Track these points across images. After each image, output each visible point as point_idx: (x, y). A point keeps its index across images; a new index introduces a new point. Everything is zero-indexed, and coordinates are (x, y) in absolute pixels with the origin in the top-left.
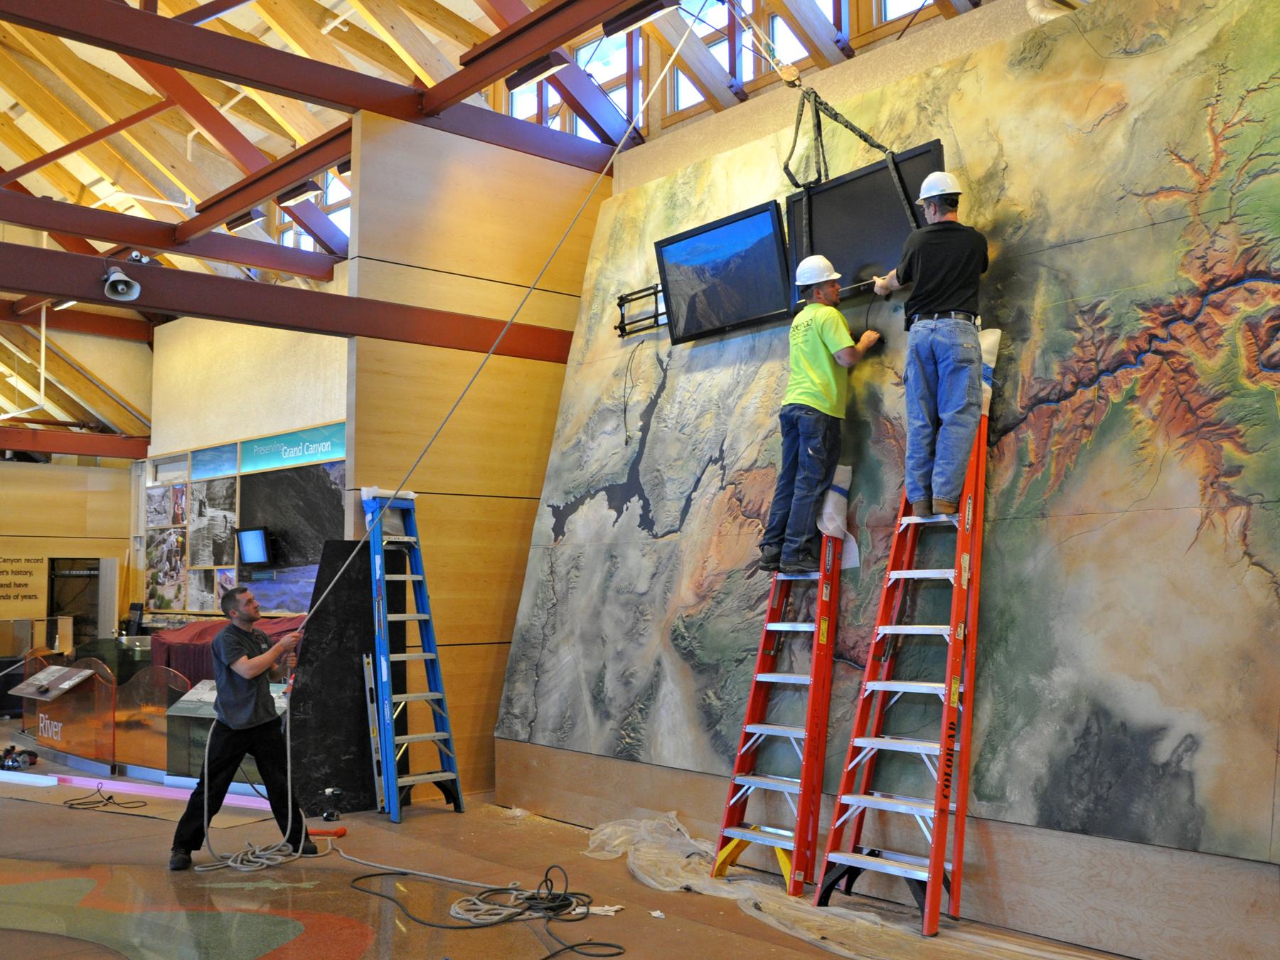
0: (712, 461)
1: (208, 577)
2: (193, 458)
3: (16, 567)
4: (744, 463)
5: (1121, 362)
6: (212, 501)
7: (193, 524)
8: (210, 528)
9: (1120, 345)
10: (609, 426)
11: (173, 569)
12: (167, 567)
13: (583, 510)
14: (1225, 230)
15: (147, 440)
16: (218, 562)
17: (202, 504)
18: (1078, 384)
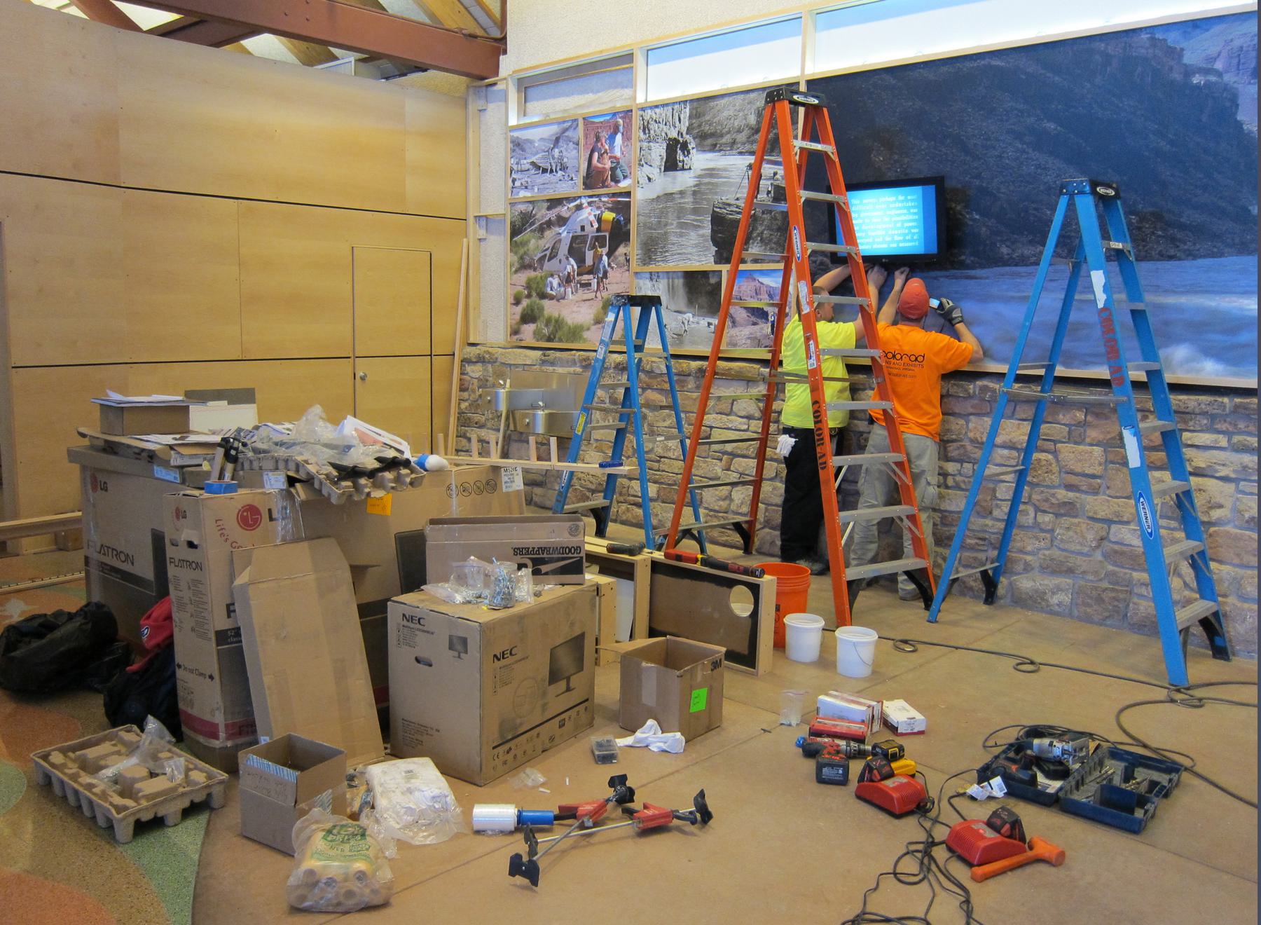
1: (700, 289)
6: (710, 139)
7: (646, 185)
17: (674, 147)
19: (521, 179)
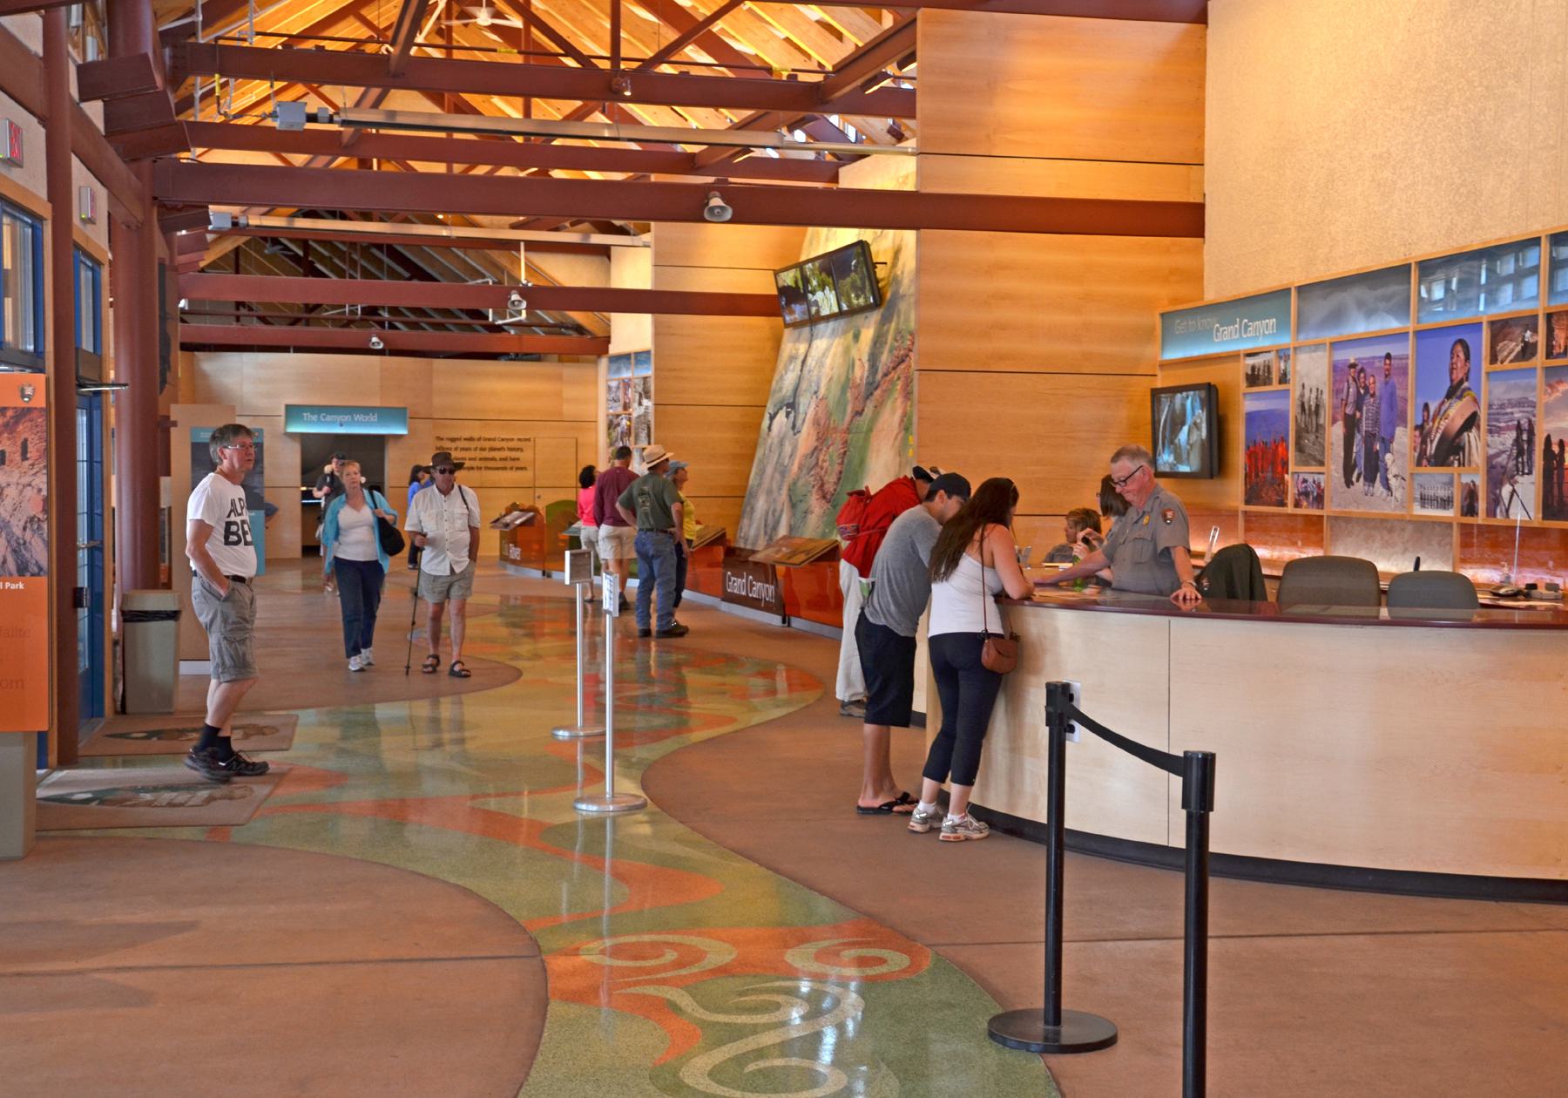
3: (511, 444)
7: (636, 411)
15: (607, 340)
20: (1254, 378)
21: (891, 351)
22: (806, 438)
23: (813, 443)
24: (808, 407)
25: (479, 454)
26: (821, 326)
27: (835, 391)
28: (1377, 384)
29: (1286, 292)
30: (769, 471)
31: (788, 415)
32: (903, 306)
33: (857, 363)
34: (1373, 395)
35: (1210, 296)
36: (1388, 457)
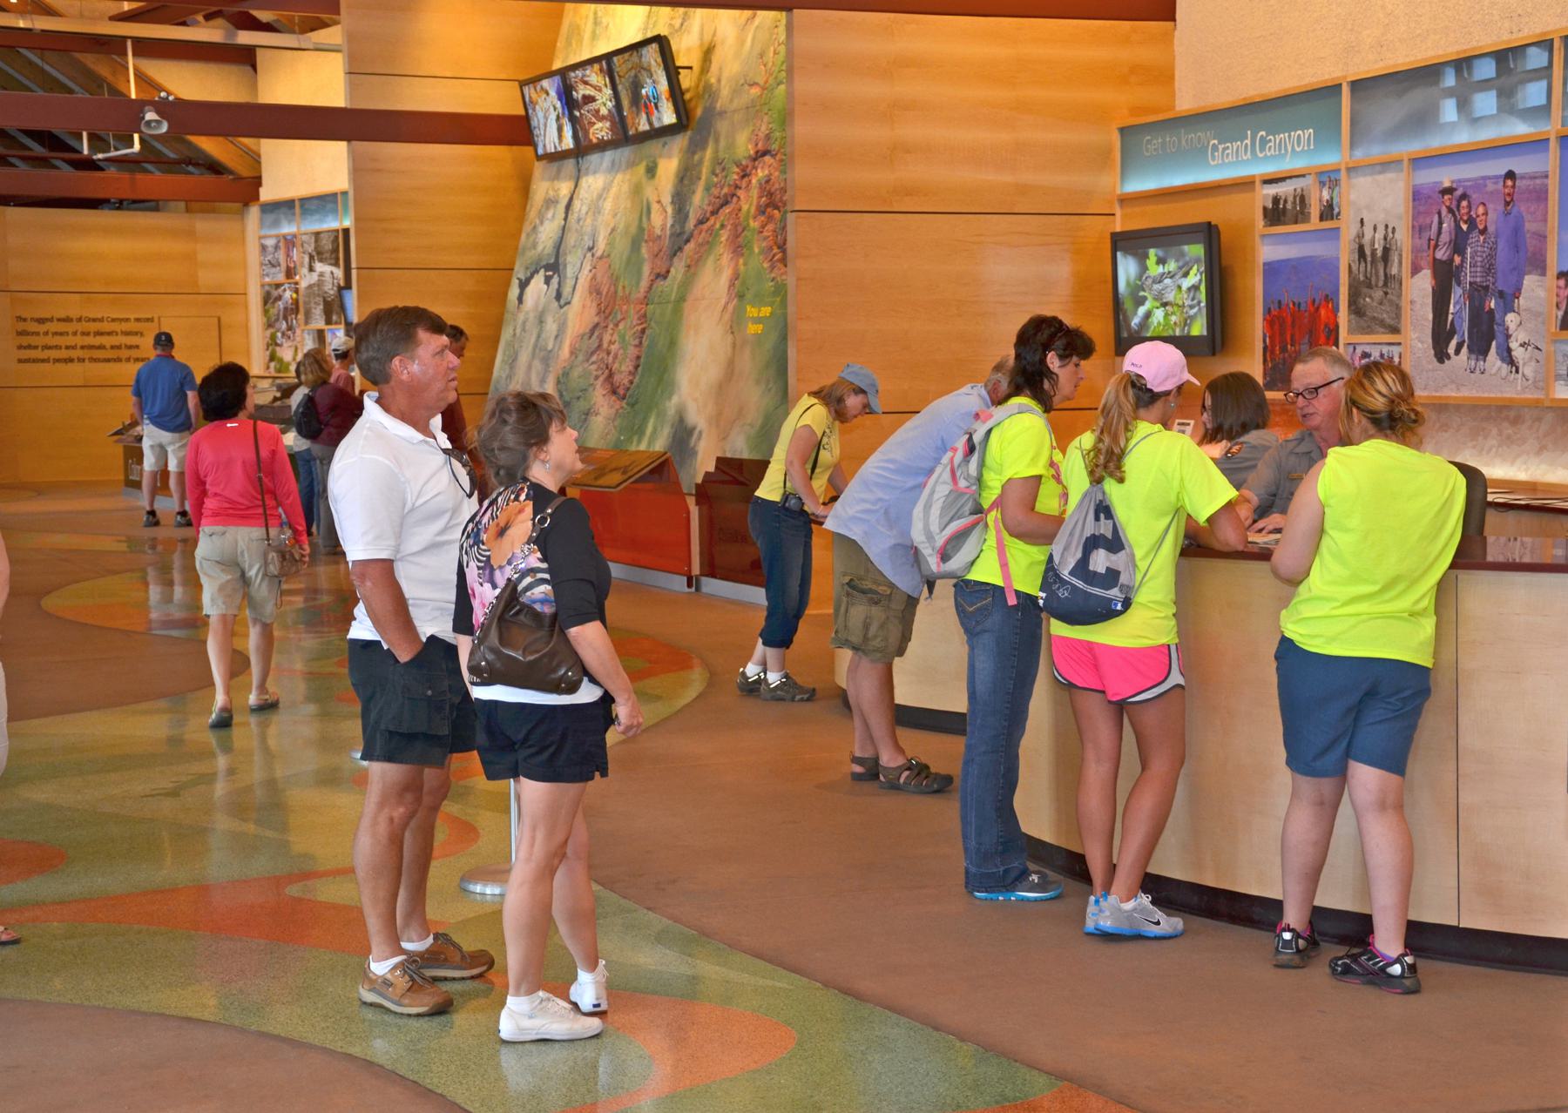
0: (590, 249)
2: (302, 206)
3: (125, 327)
4: (599, 254)
5: (726, 203)
6: (318, 255)
7: (305, 279)
8: (320, 284)
9: (725, 190)
10: (550, 215)
11: (290, 328)
12: (284, 326)
13: (533, 282)
14: (766, 119)
15: (257, 181)
16: (329, 322)
17: (311, 257)
18: (713, 213)
19: (268, 269)
20: (1276, 214)
21: (707, 189)
22: (580, 313)
23: (591, 317)
24: (578, 269)
25: (79, 340)
26: (594, 158)
27: (622, 246)
28: (1492, 216)
29: (1333, 90)
30: (524, 358)
31: (548, 281)
32: (722, 126)
33: (655, 207)
34: (1484, 231)
35: (1186, 102)
36: (1511, 319)
